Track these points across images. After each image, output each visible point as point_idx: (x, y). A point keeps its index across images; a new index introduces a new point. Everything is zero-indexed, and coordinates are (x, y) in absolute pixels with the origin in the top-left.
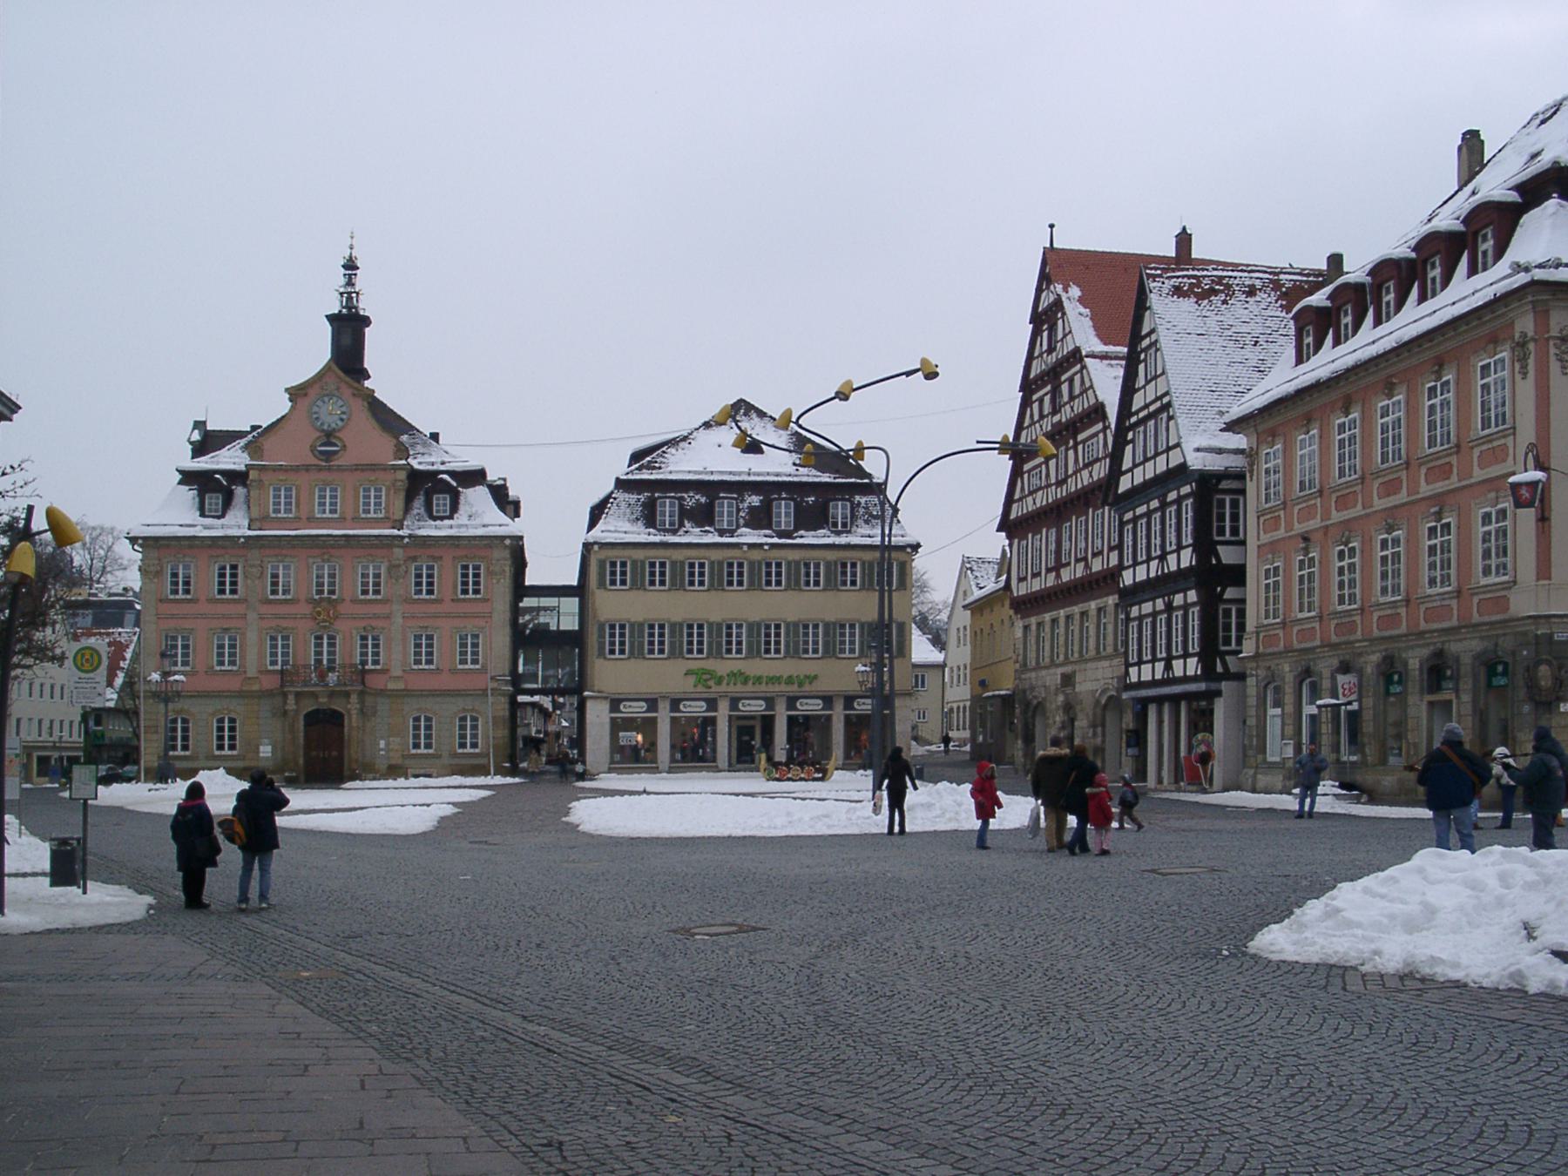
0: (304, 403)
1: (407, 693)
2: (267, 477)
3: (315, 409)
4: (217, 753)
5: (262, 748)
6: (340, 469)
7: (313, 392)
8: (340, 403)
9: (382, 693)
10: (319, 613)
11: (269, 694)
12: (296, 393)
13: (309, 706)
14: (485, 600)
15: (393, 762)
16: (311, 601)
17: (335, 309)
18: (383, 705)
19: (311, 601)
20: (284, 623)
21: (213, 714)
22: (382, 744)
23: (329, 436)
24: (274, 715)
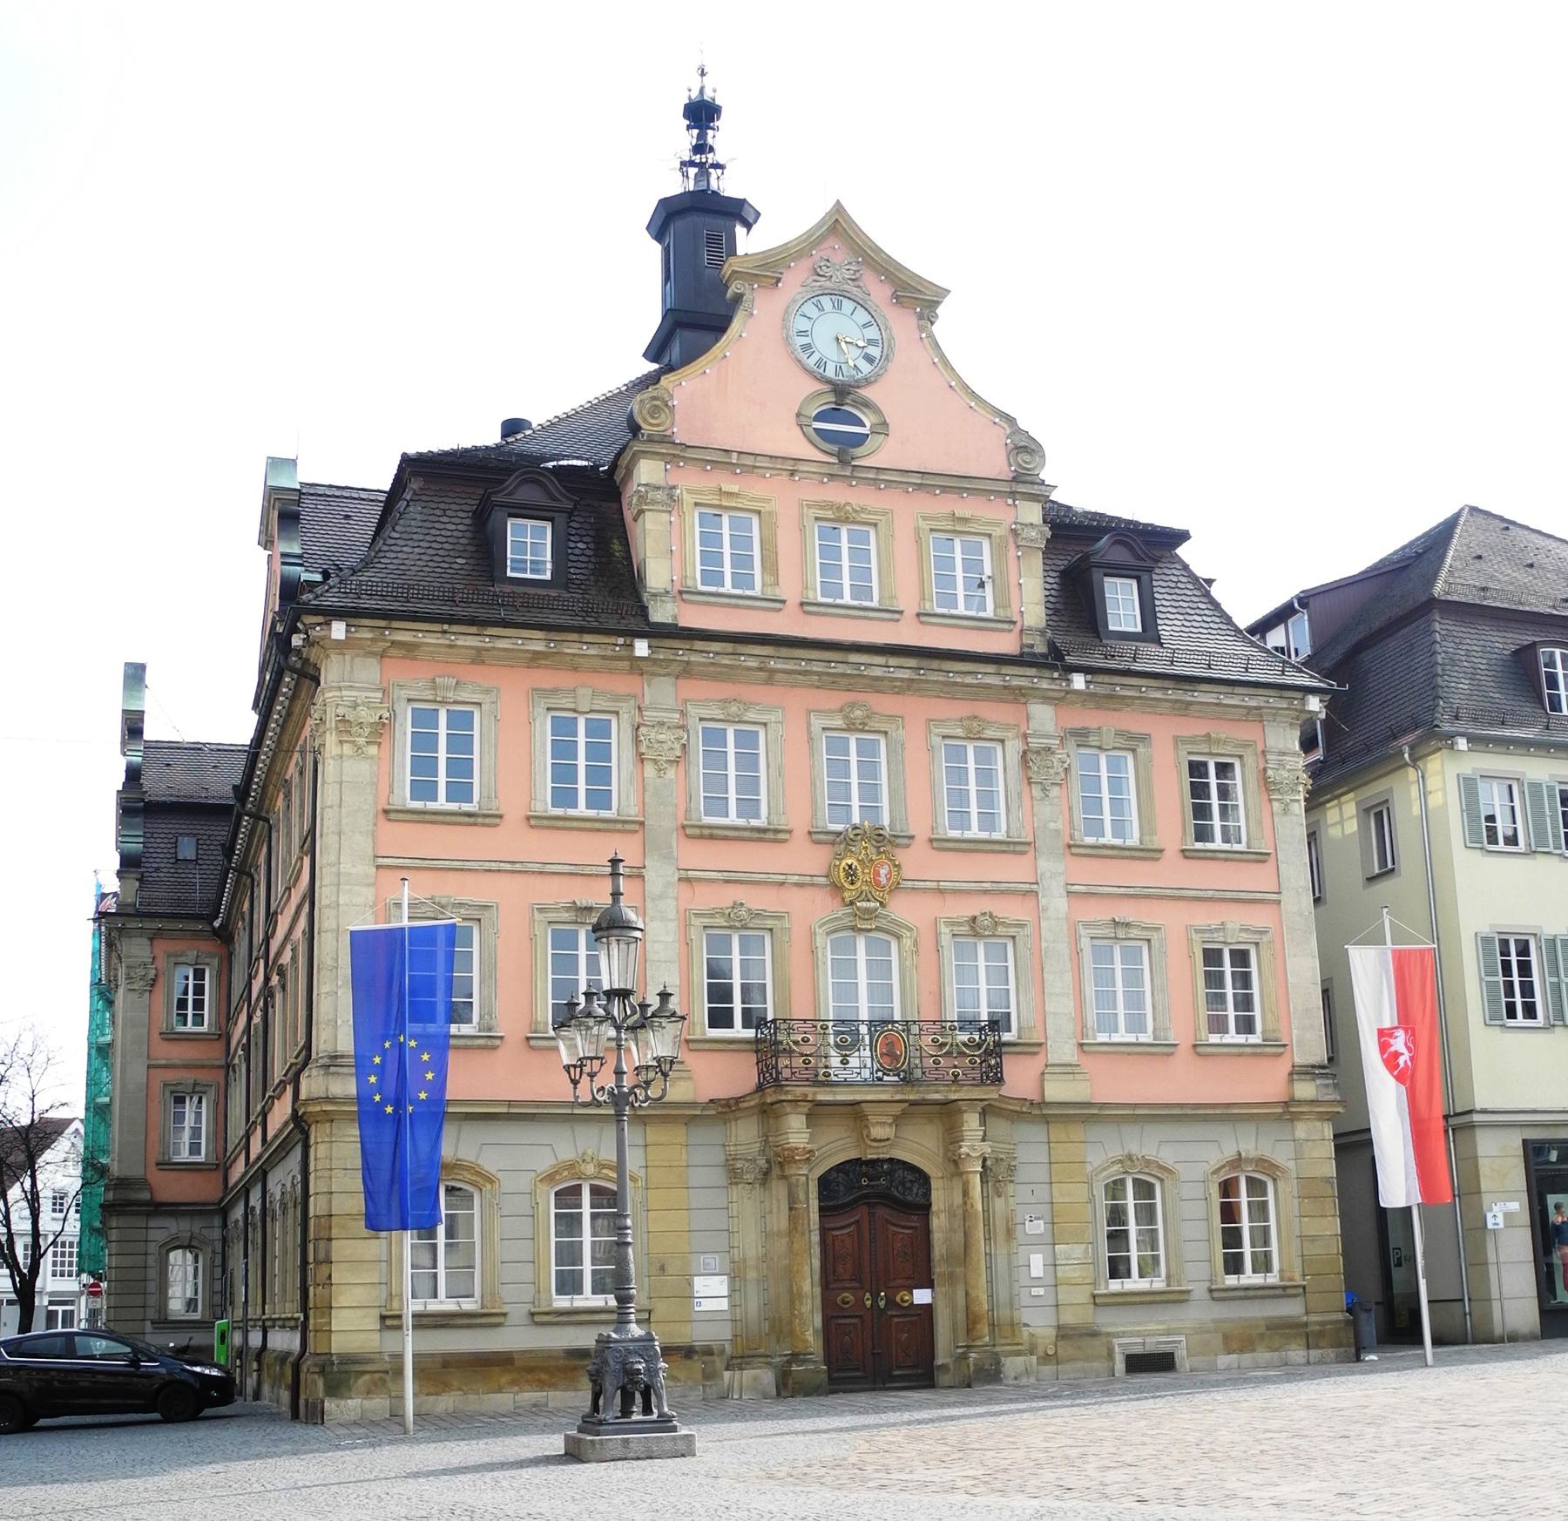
1: (1087, 1115)
2: (689, 482)
3: (803, 324)
4: (562, 1302)
5: (702, 1285)
6: (880, 478)
9: (1039, 1112)
10: (851, 872)
11: (726, 1109)
13: (837, 1147)
14: (1261, 858)
15: (1068, 1318)
16: (816, 836)
17: (675, 185)
18: (1030, 1149)
19: (816, 836)
20: (756, 899)
21: (550, 1178)
22: (1038, 1264)
24: (734, 1175)
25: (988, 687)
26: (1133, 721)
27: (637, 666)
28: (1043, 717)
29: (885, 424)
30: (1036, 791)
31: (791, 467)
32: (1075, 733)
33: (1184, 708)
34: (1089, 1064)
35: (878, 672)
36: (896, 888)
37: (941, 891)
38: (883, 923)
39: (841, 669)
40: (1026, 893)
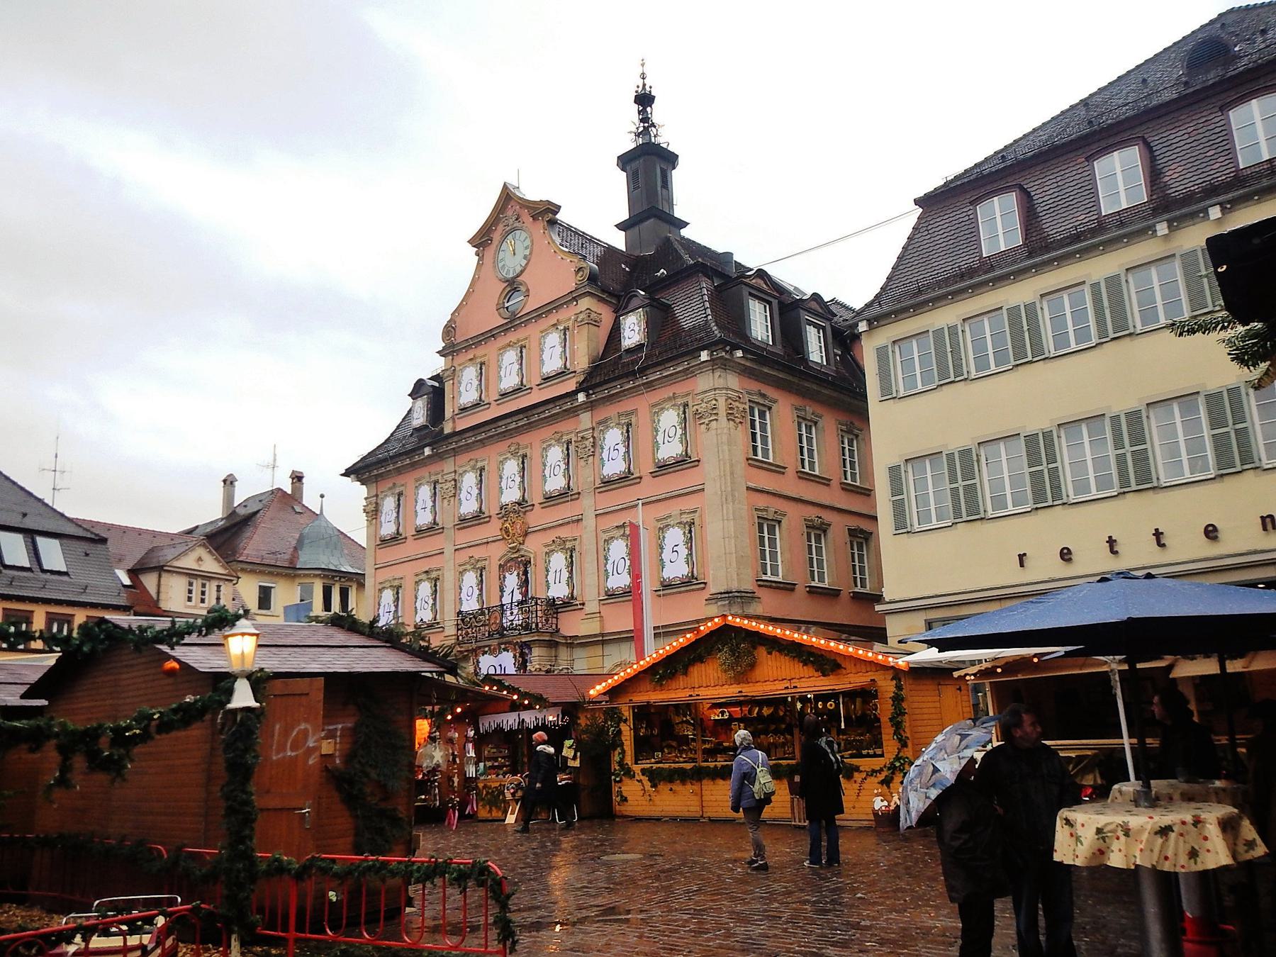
0: (489, 252)
7: (496, 236)
8: (524, 235)
12: (482, 240)
23: (513, 285)
25: (557, 414)
26: (626, 405)
27: (437, 457)
28: (586, 420)
29: (528, 290)
30: (582, 463)
31: (491, 335)
32: (599, 423)
33: (650, 386)
34: (603, 609)
35: (513, 426)
36: (526, 534)
37: (544, 529)
38: (522, 553)
39: (500, 430)
40: (578, 521)
